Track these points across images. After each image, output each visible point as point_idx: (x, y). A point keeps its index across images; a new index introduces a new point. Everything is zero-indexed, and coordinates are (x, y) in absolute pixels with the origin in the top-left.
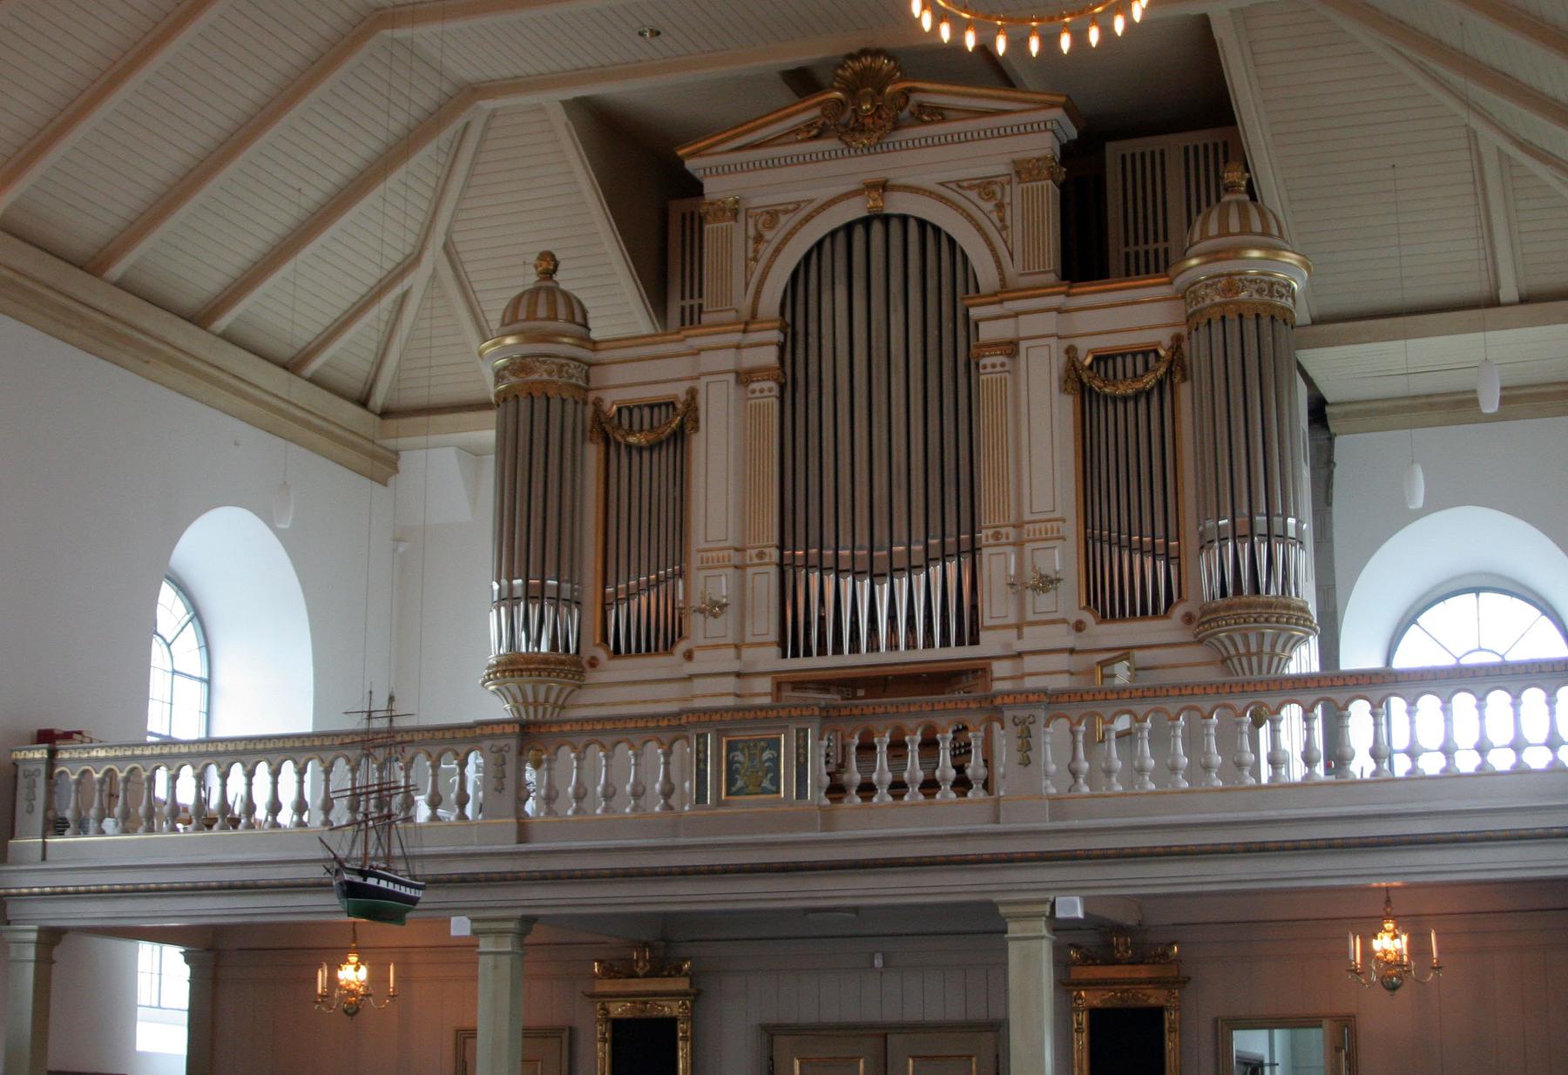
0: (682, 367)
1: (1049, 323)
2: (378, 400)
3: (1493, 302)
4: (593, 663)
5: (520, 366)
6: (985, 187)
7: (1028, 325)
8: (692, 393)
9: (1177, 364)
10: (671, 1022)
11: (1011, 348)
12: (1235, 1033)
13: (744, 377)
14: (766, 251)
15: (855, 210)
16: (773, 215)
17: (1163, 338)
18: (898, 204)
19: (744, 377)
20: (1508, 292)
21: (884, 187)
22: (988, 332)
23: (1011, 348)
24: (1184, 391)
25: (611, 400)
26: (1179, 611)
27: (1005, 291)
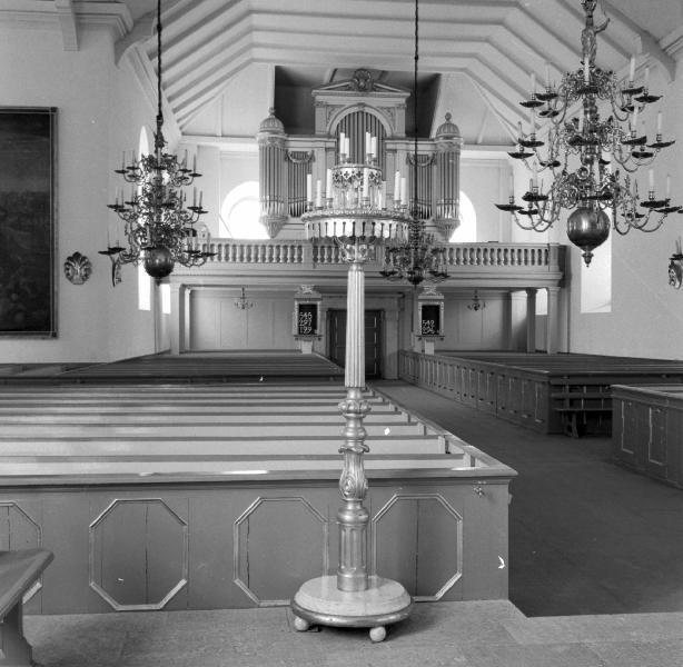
0: (310, 144)
1: (404, 146)
2: (184, 130)
3: (476, 144)
4: (287, 218)
5: (271, 139)
6: (388, 109)
7: (398, 147)
8: (313, 152)
9: (433, 161)
10: (423, 307)
11: (395, 151)
12: (582, 311)
13: (327, 149)
14: (333, 117)
15: (356, 109)
16: (334, 107)
17: (430, 154)
18: (367, 110)
19: (327, 149)
20: (480, 141)
21: (364, 105)
22: (389, 146)
23: (395, 151)
24: (435, 168)
25: (291, 150)
26: (431, 218)
27: (393, 138)
